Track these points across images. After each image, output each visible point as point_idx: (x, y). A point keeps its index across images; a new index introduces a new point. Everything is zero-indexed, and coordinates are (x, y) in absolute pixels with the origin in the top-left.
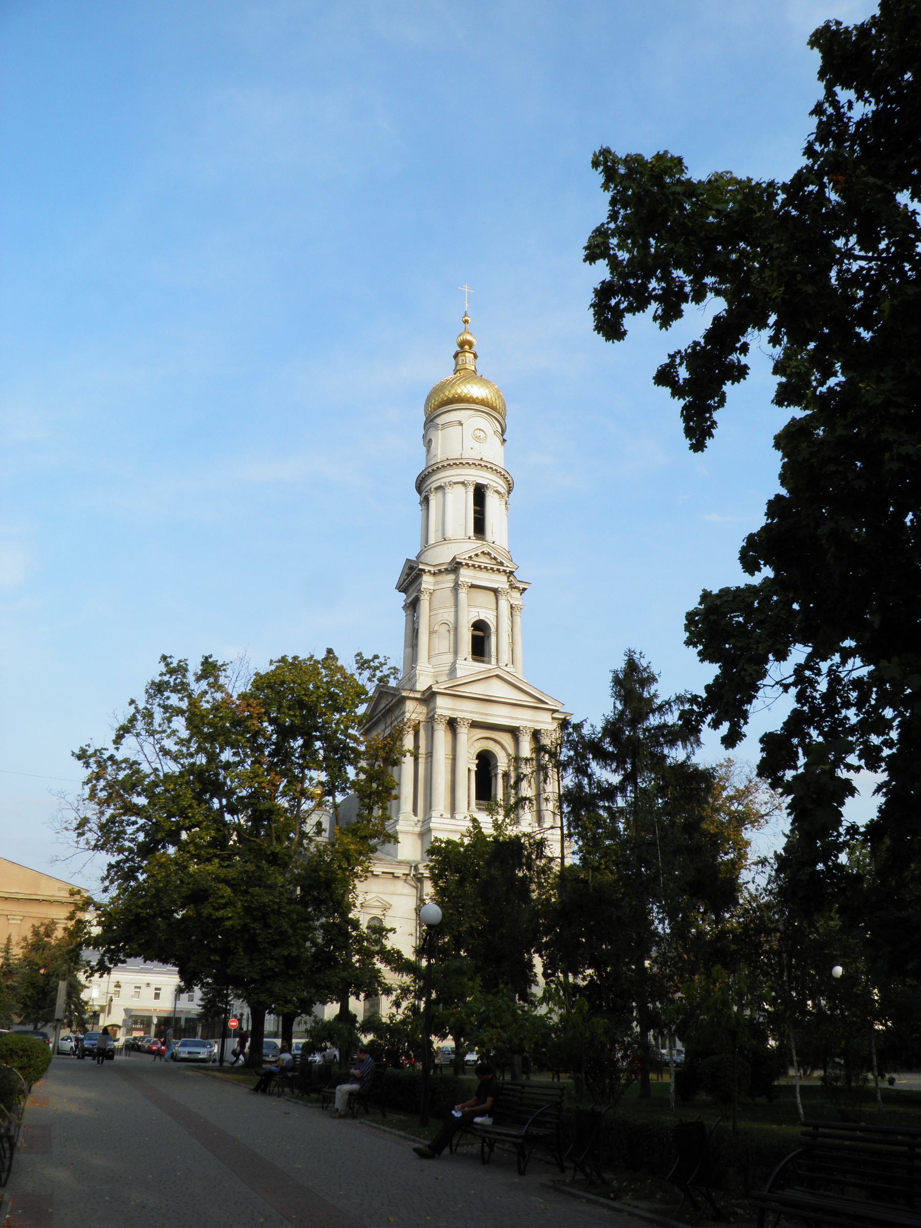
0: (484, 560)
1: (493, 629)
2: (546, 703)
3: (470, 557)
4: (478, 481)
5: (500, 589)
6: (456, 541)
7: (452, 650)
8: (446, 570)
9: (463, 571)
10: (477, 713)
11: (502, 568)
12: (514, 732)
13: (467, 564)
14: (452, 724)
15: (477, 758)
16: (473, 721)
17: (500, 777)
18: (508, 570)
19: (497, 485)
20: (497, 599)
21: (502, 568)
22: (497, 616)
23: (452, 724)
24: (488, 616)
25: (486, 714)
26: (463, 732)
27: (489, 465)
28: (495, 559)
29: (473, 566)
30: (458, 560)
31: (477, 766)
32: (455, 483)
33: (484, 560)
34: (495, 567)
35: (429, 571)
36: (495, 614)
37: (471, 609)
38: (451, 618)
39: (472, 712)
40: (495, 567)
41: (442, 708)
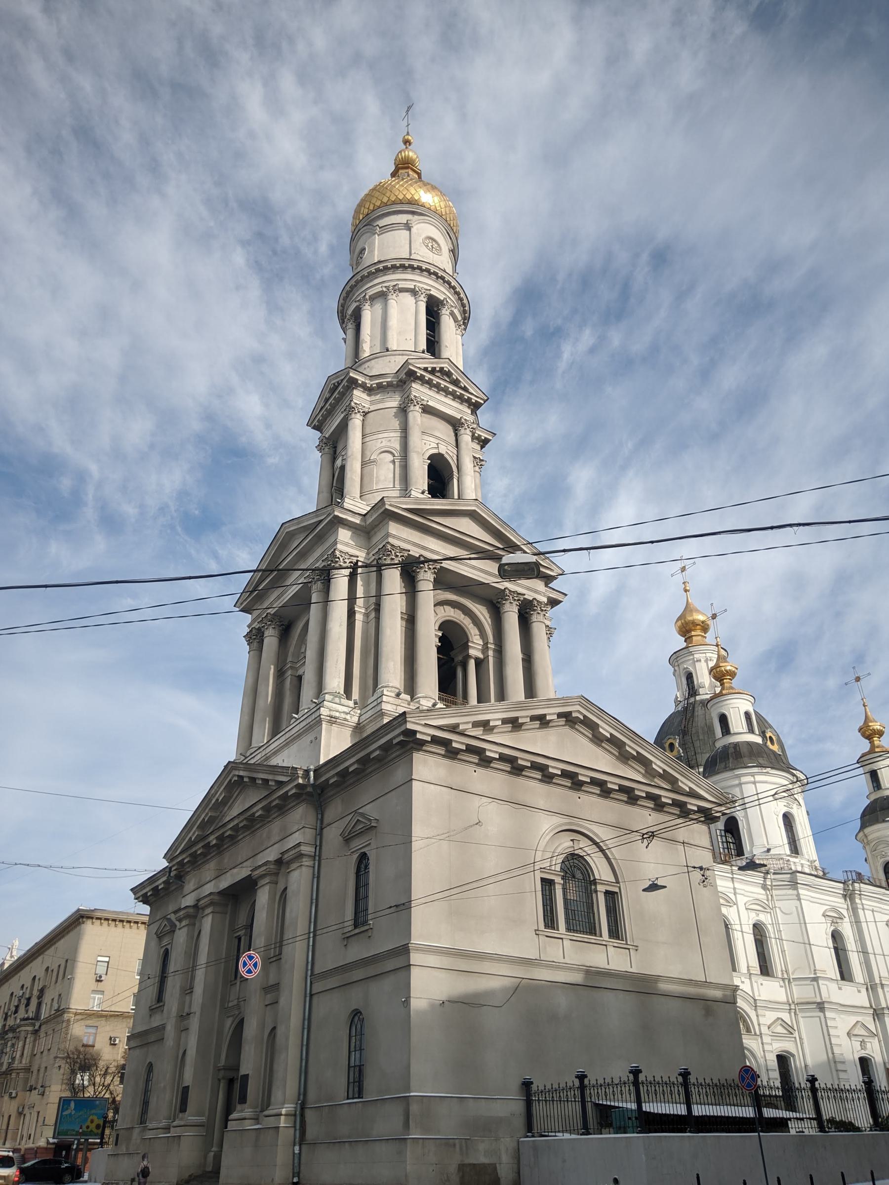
3: (425, 369)
4: (432, 292)
8: (390, 384)
17: (472, 664)
18: (474, 399)
21: (467, 395)
24: (447, 450)
34: (459, 391)
38: (396, 445)
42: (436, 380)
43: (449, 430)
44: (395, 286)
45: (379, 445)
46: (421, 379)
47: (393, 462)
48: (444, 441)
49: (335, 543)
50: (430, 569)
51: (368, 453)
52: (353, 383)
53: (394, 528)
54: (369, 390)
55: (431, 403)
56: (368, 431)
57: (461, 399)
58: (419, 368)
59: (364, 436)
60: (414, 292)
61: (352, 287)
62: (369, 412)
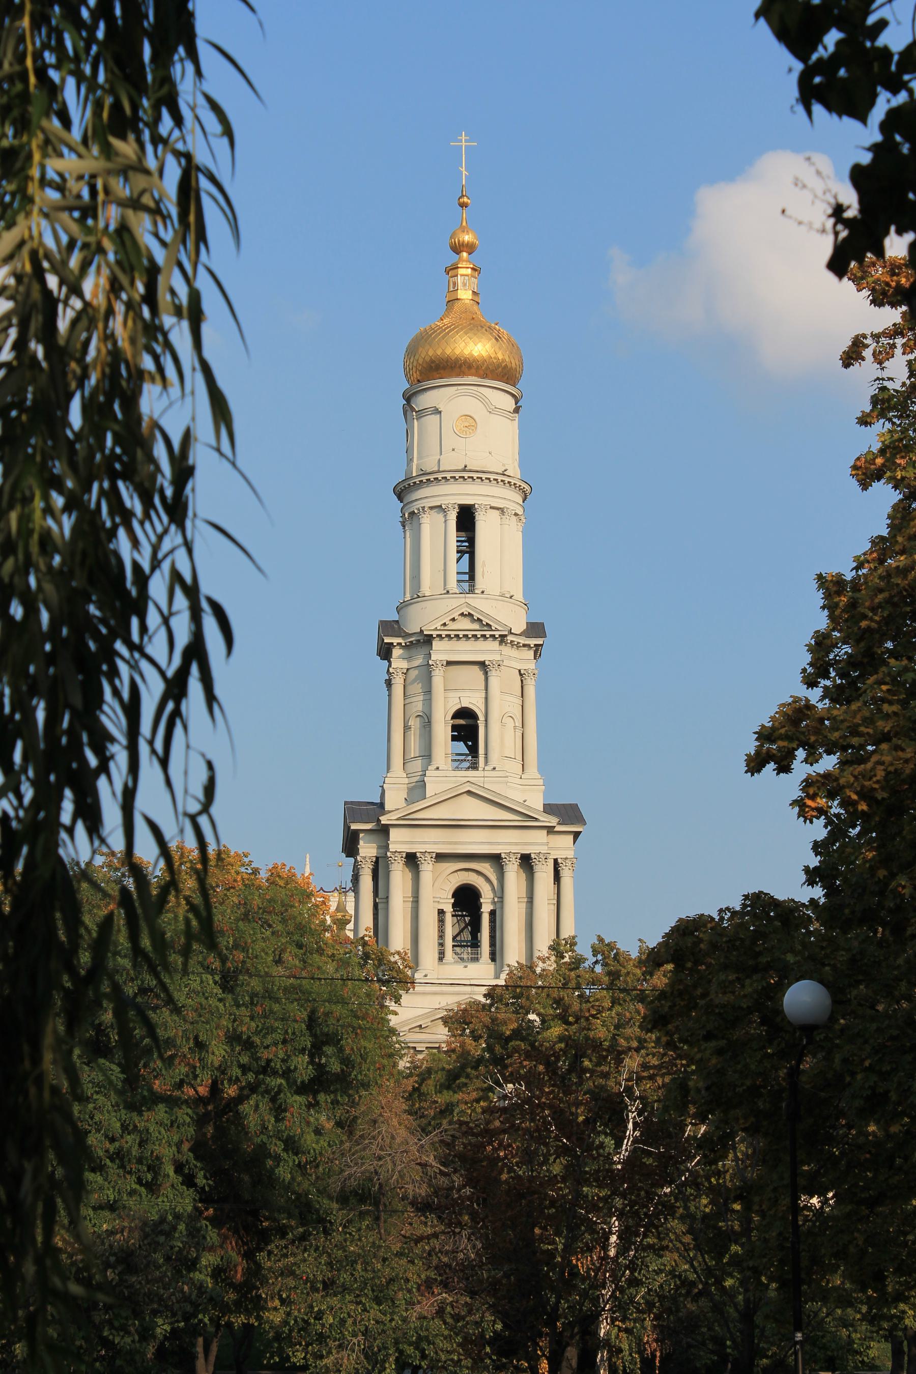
0: (465, 624)
1: (481, 718)
2: (536, 820)
6: (432, 598)
9: (436, 644)
10: (444, 843)
11: (488, 633)
12: (496, 859)
13: (439, 636)
14: (412, 860)
15: (453, 896)
16: (437, 854)
22: (486, 698)
23: (412, 860)
24: (474, 702)
25: (456, 843)
26: (427, 868)
28: (479, 620)
29: (448, 636)
30: (425, 633)
33: (466, 624)
35: (399, 644)
37: (451, 694)
39: (435, 843)
40: (479, 634)
41: (395, 842)
58: (436, 629)
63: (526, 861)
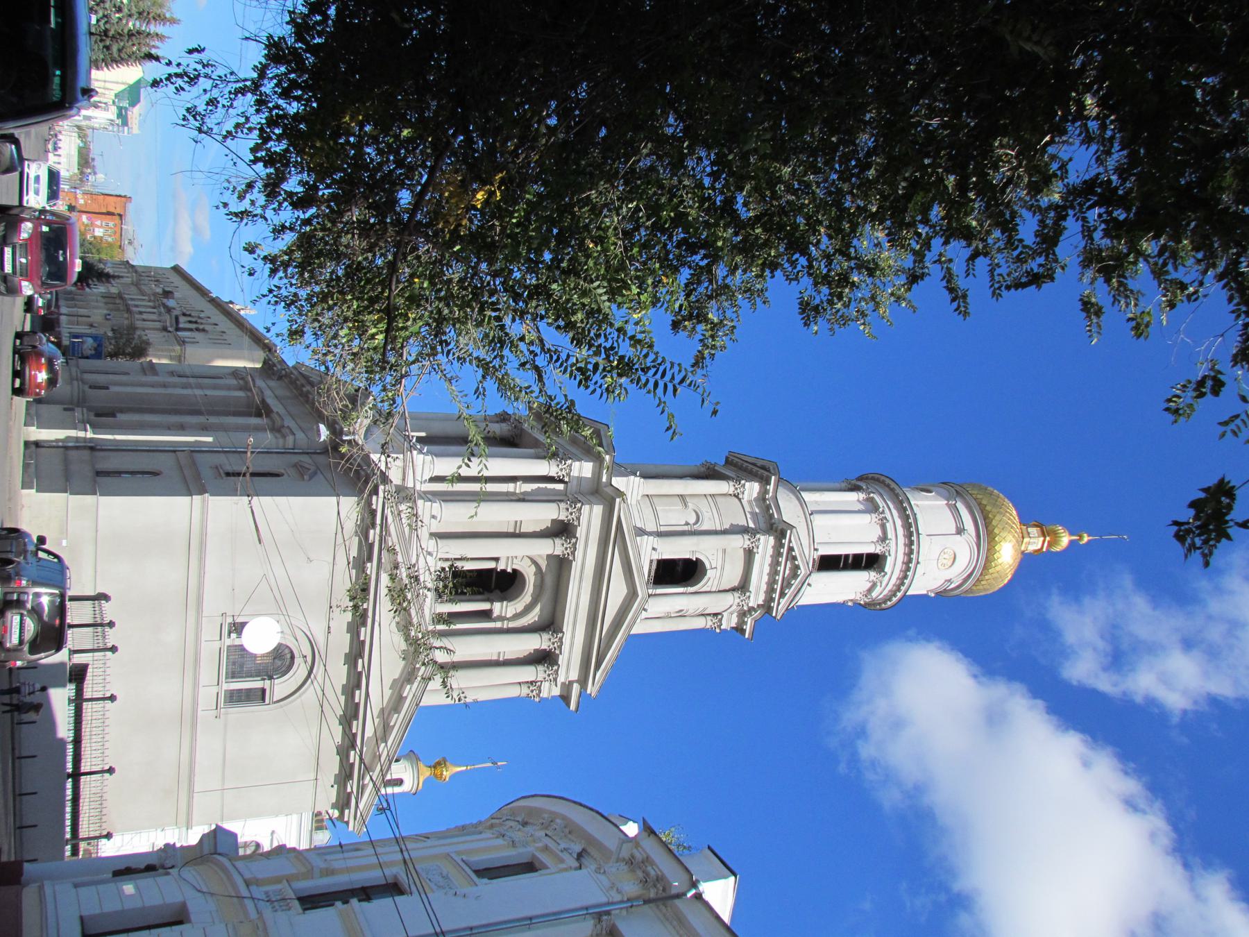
1: (690, 589)
3: (791, 549)
5: (748, 594)
7: (663, 529)
8: (772, 516)
11: (776, 596)
12: (551, 624)
15: (515, 571)
17: (484, 606)
18: (774, 605)
19: (883, 585)
20: (733, 590)
21: (776, 596)
23: (562, 530)
24: (711, 580)
26: (556, 547)
27: (910, 574)
28: (789, 585)
31: (504, 571)
32: (883, 527)
33: (784, 569)
34: (778, 587)
35: (766, 492)
36: (714, 590)
38: (705, 526)
42: (782, 560)
43: (736, 583)
44: (885, 518)
45: (704, 510)
46: (779, 545)
47: (687, 524)
48: (721, 575)
49: (580, 460)
50: (566, 549)
51: (695, 500)
52: (765, 481)
53: (598, 510)
54: (762, 498)
55: (757, 558)
56: (719, 500)
57: (770, 590)
58: (790, 541)
59: (712, 496)
60: (884, 538)
61: (878, 480)
62: (740, 500)
63: (545, 658)
